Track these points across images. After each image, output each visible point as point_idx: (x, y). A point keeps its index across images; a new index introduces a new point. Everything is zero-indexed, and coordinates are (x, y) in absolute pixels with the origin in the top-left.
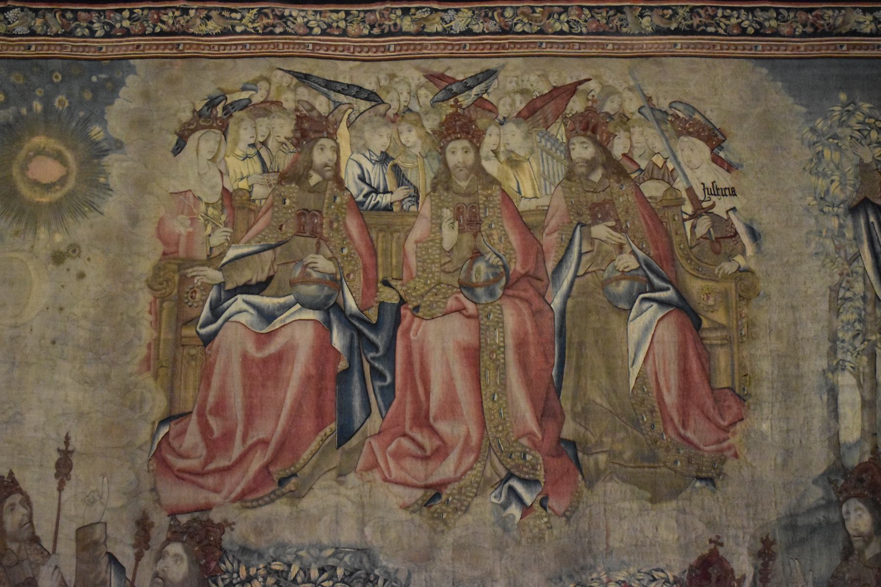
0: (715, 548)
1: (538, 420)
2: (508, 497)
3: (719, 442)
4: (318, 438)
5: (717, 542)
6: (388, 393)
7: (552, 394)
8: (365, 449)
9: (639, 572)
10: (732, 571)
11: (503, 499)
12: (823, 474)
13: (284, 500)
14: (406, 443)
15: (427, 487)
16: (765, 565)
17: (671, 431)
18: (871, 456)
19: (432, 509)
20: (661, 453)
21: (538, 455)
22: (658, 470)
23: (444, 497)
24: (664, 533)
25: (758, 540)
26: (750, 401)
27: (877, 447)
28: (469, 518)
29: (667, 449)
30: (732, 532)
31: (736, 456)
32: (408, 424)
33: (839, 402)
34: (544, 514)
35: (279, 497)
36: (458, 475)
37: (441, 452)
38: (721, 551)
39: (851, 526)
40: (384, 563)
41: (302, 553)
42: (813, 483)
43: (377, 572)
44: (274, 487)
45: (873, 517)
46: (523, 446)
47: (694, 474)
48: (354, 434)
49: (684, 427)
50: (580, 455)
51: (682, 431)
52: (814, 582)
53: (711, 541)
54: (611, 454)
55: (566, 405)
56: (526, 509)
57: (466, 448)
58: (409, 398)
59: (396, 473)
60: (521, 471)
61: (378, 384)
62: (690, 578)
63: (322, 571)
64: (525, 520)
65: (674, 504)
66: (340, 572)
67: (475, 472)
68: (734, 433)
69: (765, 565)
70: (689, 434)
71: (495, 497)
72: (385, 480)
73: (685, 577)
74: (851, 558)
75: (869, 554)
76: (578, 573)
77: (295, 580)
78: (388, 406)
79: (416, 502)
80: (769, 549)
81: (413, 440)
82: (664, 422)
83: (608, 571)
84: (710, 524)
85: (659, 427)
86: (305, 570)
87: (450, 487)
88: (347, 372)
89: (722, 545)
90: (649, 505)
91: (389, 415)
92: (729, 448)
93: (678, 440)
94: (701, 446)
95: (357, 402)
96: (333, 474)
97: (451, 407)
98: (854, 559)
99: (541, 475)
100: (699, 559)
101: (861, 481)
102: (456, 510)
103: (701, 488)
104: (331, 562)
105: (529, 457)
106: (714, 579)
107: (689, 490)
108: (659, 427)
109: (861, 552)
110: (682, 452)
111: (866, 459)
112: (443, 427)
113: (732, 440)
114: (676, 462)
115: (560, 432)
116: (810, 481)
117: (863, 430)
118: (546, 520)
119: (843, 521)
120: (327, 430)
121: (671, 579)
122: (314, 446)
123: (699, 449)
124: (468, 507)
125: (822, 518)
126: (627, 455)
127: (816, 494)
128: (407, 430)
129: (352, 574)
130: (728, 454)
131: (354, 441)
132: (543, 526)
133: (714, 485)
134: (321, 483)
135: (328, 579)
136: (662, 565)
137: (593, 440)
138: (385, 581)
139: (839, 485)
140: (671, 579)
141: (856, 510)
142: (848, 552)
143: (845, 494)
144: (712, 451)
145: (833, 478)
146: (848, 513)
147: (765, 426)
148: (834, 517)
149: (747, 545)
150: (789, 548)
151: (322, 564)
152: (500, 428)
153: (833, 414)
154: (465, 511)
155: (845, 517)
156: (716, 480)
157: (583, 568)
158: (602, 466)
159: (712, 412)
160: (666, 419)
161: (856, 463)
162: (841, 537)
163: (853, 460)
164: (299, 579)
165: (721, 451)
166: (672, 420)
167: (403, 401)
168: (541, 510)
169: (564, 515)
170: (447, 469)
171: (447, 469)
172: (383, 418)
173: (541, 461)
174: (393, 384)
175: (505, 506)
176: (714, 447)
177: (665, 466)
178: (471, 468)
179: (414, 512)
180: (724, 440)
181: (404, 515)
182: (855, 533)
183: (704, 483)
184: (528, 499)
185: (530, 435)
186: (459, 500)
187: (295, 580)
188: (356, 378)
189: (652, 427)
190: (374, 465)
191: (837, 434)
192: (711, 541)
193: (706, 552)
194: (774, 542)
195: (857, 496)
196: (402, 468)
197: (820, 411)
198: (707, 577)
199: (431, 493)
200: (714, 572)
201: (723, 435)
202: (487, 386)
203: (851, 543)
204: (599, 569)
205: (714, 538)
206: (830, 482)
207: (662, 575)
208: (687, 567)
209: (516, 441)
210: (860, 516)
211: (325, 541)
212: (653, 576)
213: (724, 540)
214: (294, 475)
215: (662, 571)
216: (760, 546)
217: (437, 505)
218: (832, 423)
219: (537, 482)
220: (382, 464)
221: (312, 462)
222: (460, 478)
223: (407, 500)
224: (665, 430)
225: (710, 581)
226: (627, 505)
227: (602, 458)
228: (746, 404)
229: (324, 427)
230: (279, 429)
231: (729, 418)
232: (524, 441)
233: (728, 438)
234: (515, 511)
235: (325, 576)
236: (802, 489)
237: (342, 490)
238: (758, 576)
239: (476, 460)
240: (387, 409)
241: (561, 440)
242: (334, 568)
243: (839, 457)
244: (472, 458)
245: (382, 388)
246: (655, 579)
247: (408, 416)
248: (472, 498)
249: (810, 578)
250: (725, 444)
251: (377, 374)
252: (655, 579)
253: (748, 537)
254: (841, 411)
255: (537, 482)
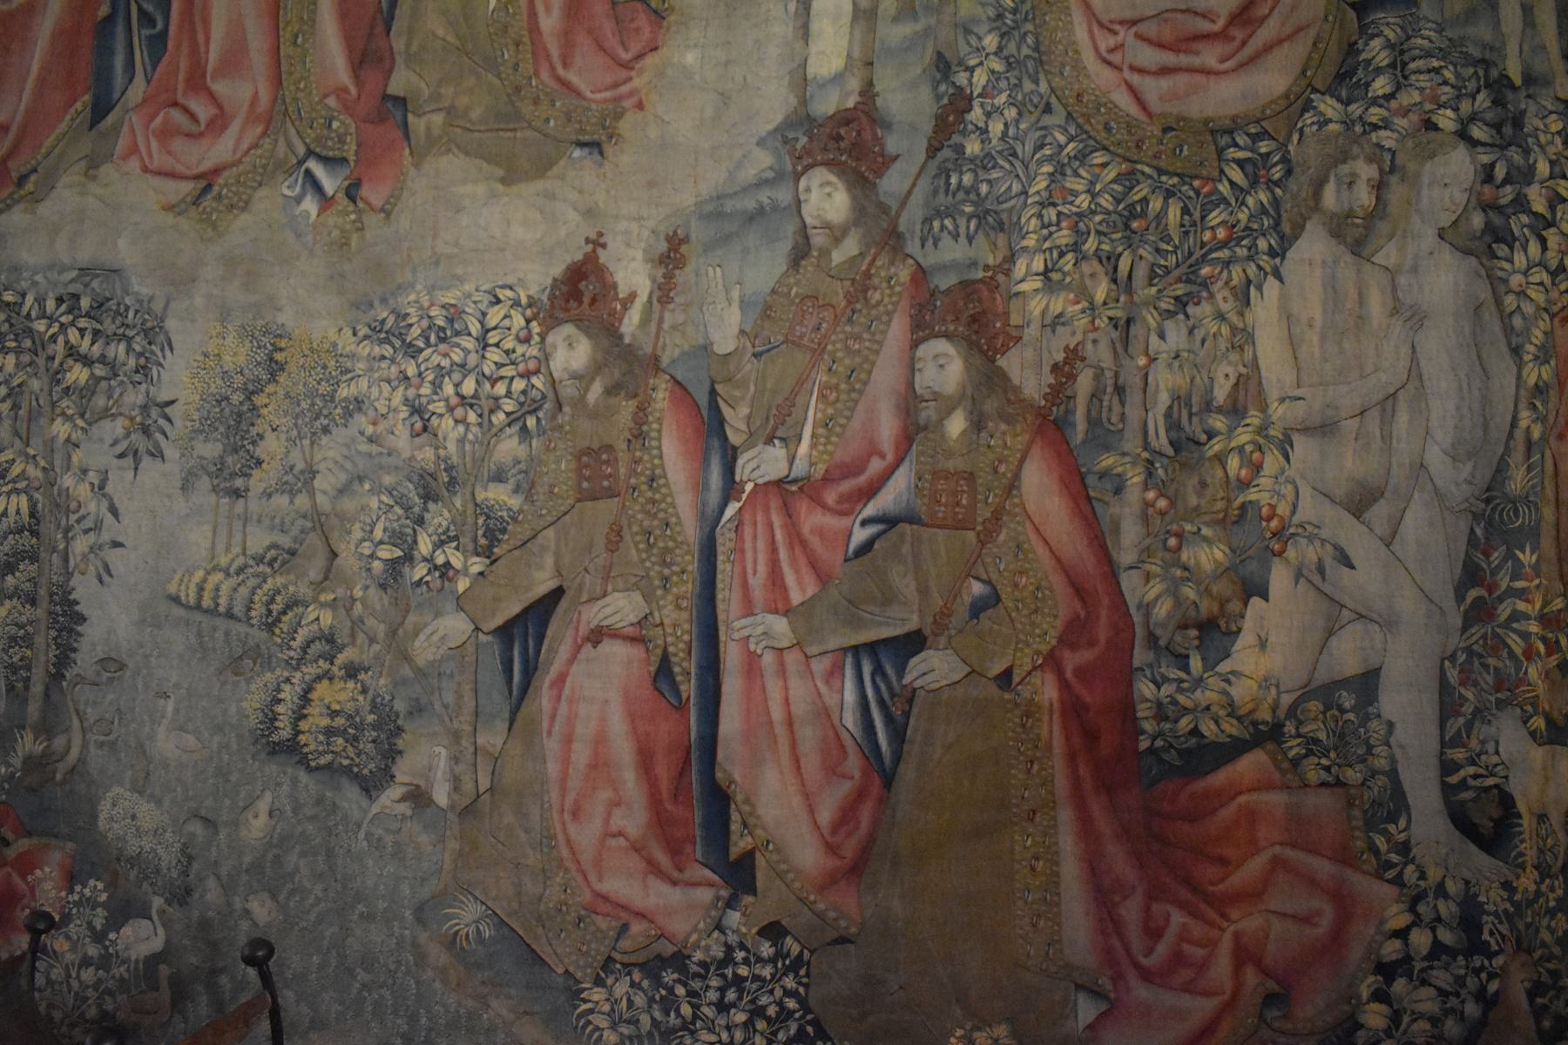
0: (594, 251)
1: (354, 71)
2: (303, 187)
3: (616, 85)
4: (68, 117)
5: (598, 243)
6: (158, 44)
7: (380, 28)
8: (125, 129)
9: (477, 290)
10: (614, 286)
11: (298, 189)
12: (776, 130)
13: (22, 206)
14: (176, 115)
15: (197, 177)
16: (669, 276)
17: (545, 74)
18: (858, 99)
19: (201, 209)
20: (526, 108)
21: (349, 121)
22: (519, 134)
23: (216, 189)
24: (518, 232)
25: (662, 237)
26: (672, 18)
27: (870, 84)
28: (245, 219)
29: (536, 102)
30: (622, 225)
31: (640, 106)
32: (181, 86)
33: (813, 12)
34: (351, 208)
35: (18, 202)
36: (238, 155)
37: (219, 123)
38: (603, 256)
39: (809, 213)
40: (136, 288)
41: (38, 278)
42: (758, 144)
43: (128, 301)
44: (12, 188)
45: (854, 198)
46: (330, 108)
47: (573, 137)
48: (113, 107)
49: (565, 65)
50: (410, 117)
51: (561, 71)
52: (742, 301)
53: (588, 241)
54: (450, 111)
55: (398, 43)
56: (326, 201)
57: (252, 118)
58: (185, 50)
59: (159, 160)
60: (325, 147)
61: (146, 32)
62: (552, 297)
63: (60, 300)
64: (322, 219)
65: (539, 185)
66: (85, 303)
67: (259, 151)
68: (641, 71)
69: (669, 276)
70: (573, 77)
71: (289, 187)
72: (145, 170)
73: (545, 298)
74: (803, 263)
75: (837, 257)
76: (393, 294)
77: (29, 315)
78: (155, 64)
79: (183, 200)
80: (676, 251)
81: (186, 110)
82: (536, 62)
83: (431, 290)
84: (590, 213)
85: (527, 67)
86: (40, 301)
87: (226, 174)
88: (110, 19)
89: (604, 246)
90: (500, 187)
91: (156, 76)
92: (631, 94)
93: (552, 83)
94: (588, 94)
95: (119, 62)
96: (83, 163)
97: (234, 61)
98: (808, 265)
99: (350, 150)
100: (568, 268)
101: (839, 138)
102: (231, 207)
103: (581, 159)
104: (72, 289)
105: (335, 125)
106: (586, 300)
107: (562, 163)
108: (527, 67)
109: (825, 253)
110: (558, 104)
111: (850, 103)
112: (220, 87)
113: (637, 82)
114: (547, 120)
115: (386, 86)
116: (754, 141)
117: (849, 56)
118: (353, 217)
119: (798, 203)
120: (79, 105)
121: (524, 301)
122: (63, 127)
123: (585, 99)
124: (247, 203)
125: (766, 201)
126: (476, 114)
127: (763, 161)
128: (180, 99)
129: (101, 305)
130: (627, 103)
131: (110, 119)
132: (348, 227)
133: (601, 153)
134: (65, 179)
135: (69, 312)
136: (510, 280)
137: (426, 92)
138: (137, 312)
139: (799, 146)
140: (524, 301)
141: (822, 185)
142: (801, 252)
143: (807, 161)
144: (605, 101)
145: (791, 135)
146: (808, 190)
147: (691, 58)
148: (783, 196)
149: (643, 245)
150: (708, 248)
151: (61, 291)
152: (302, 85)
153: (801, 32)
154: (244, 209)
155: (802, 198)
156: (605, 146)
157: (399, 287)
158: (436, 132)
159: (612, 42)
160: (539, 51)
161: (831, 112)
162: (790, 228)
163: (827, 105)
164: (33, 314)
165: (617, 100)
166: (548, 56)
167: (177, 57)
168: (346, 201)
169: (382, 210)
170: (221, 149)
171: (221, 149)
172: (148, 82)
173: (352, 129)
174: (165, 31)
175: (299, 200)
176: (608, 94)
177: (530, 126)
178: (255, 146)
179: (179, 214)
180: (625, 82)
181: (169, 219)
182: (816, 223)
183: (586, 150)
184: (329, 184)
185: (341, 91)
186: (235, 194)
187: (29, 315)
188: (120, 29)
189: (516, 67)
190: (134, 150)
191: (804, 64)
192: (588, 241)
193: (579, 257)
194: (685, 240)
195: (827, 164)
196: (169, 153)
197: (782, 29)
198: (576, 295)
199: (203, 183)
200: (588, 288)
201: (624, 74)
202: (288, 23)
203: (807, 238)
204: (419, 287)
205: (593, 236)
206: (786, 141)
207: (509, 293)
208: (549, 281)
209: (321, 101)
210: (829, 195)
211: (66, 260)
212: (495, 296)
213: (607, 239)
214: (35, 170)
215: (511, 289)
216: (663, 246)
217: (208, 202)
218: (799, 45)
219: (344, 160)
220: (143, 148)
221: (57, 151)
222: (240, 162)
223: (173, 199)
224: (537, 74)
225: (581, 303)
226: (469, 189)
227: (438, 119)
228: (665, 23)
229: (75, 101)
230: (22, 108)
231: (635, 49)
232: (332, 102)
233: (630, 79)
234: (310, 205)
235: (63, 308)
236: (738, 154)
237: (93, 187)
238: (657, 294)
239: (264, 134)
240: (154, 69)
241: (386, 97)
242: (76, 297)
243: (804, 102)
244: (259, 129)
245: (150, 38)
246: (498, 301)
247: (182, 76)
248: (255, 189)
249: (735, 294)
250: (624, 89)
251: (147, 19)
252: (498, 301)
253: (645, 233)
254: (814, 26)
255: (344, 160)
